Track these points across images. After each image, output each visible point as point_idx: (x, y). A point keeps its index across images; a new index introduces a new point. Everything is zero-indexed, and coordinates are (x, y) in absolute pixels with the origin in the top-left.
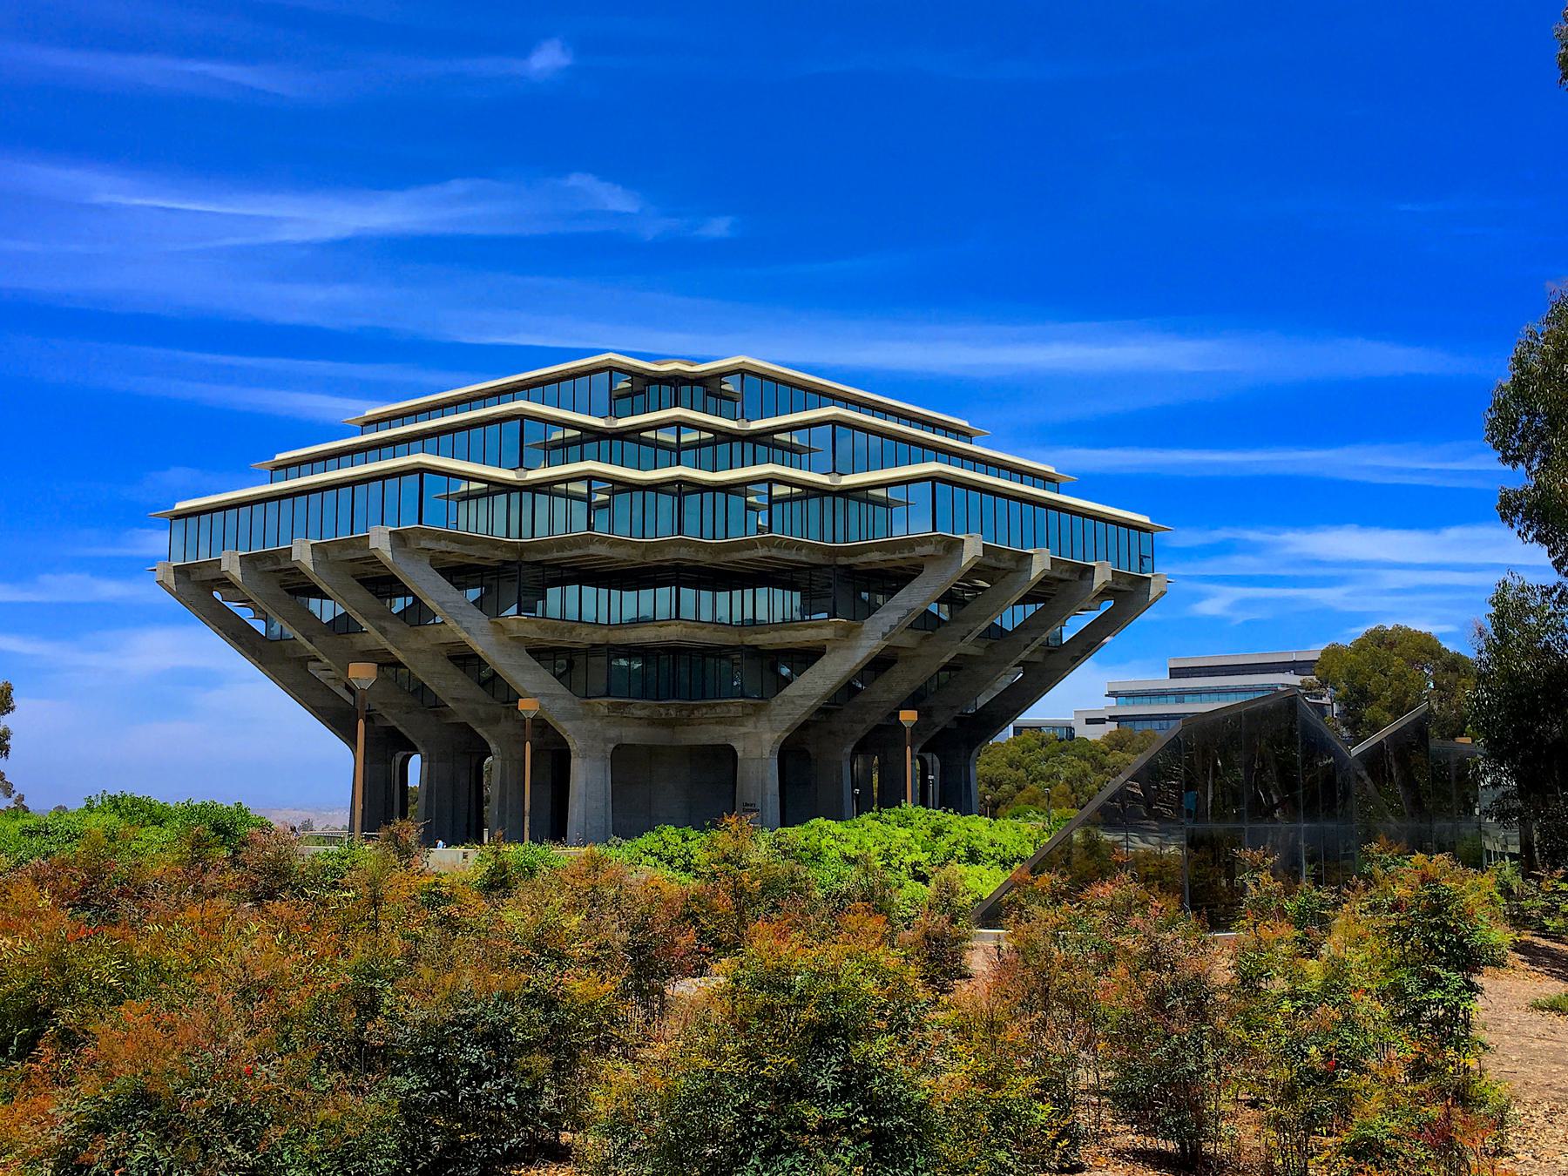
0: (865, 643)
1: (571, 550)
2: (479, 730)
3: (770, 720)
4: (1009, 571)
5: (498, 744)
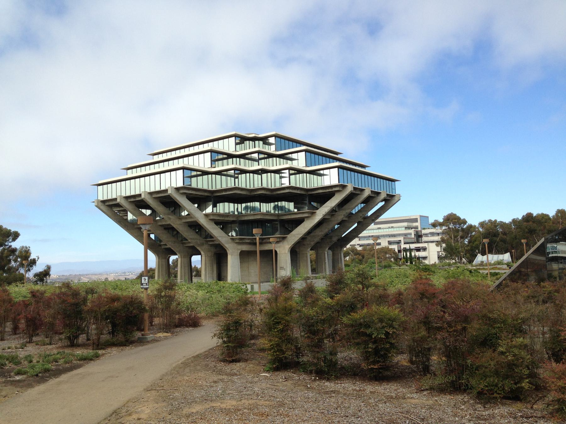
2: (198, 248)
4: (358, 194)
5: (204, 252)
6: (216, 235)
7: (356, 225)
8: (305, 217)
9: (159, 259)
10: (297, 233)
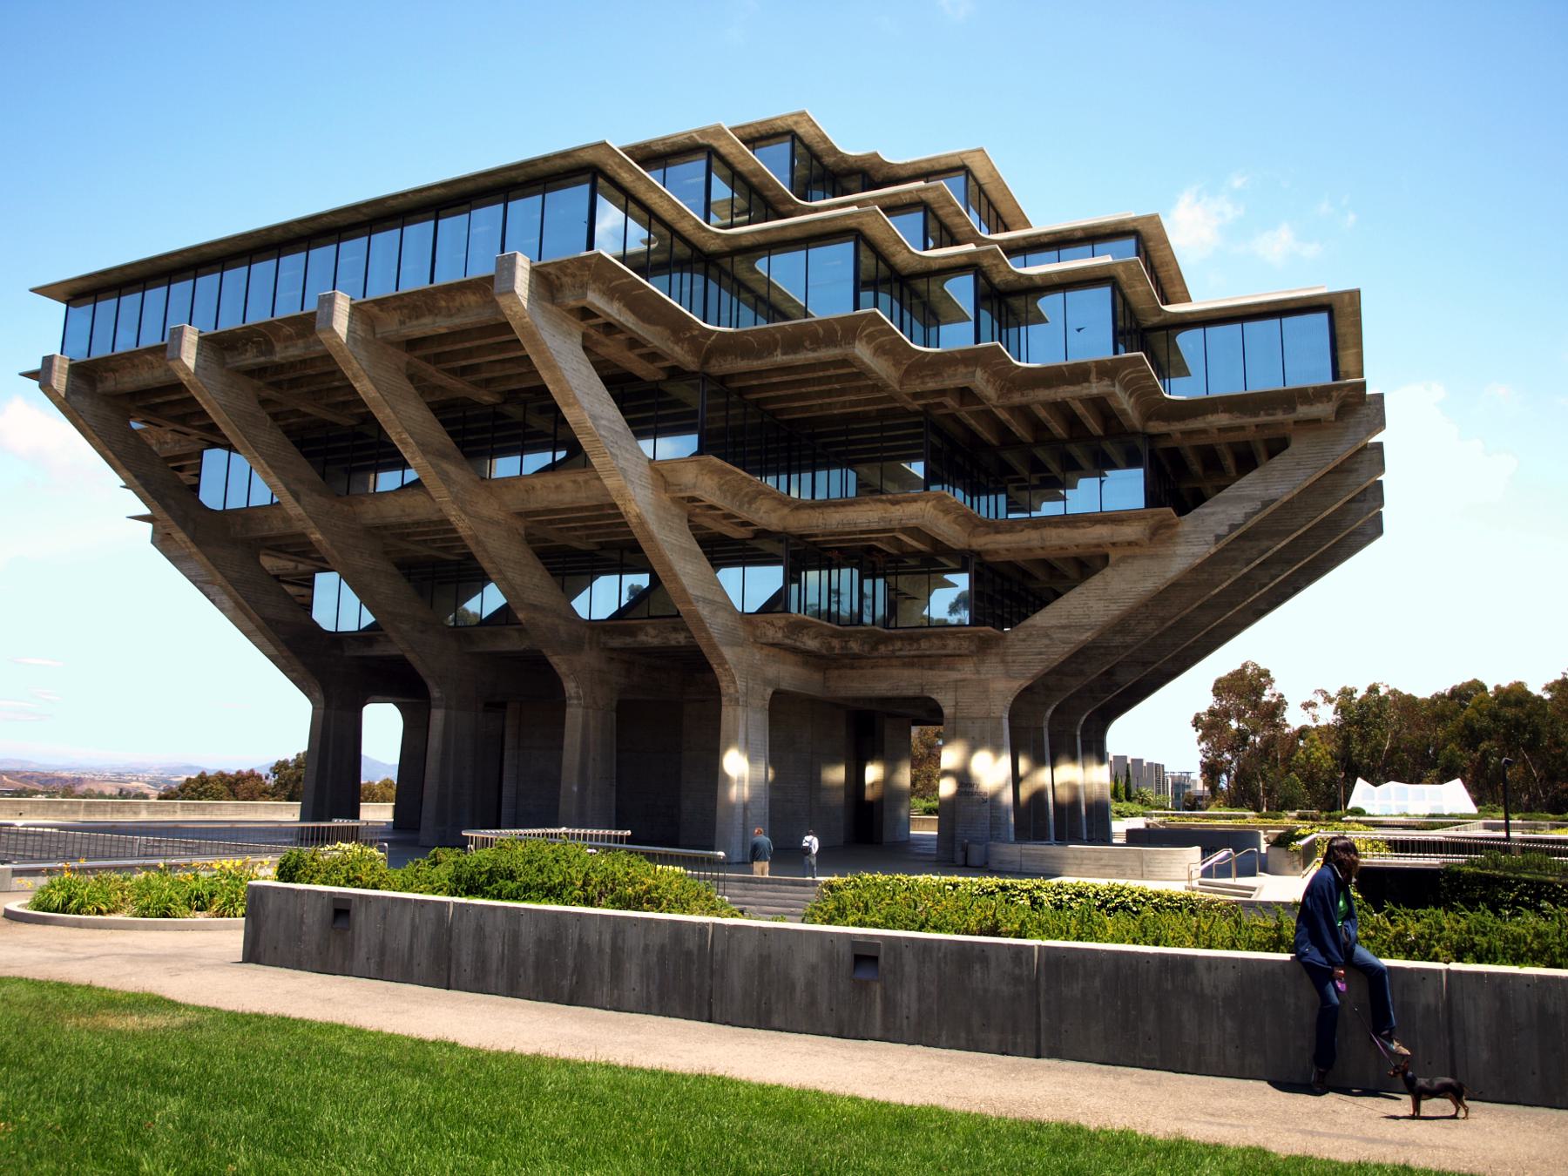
0: (1181, 549)
1: (814, 350)
3: (1003, 661)
9: (327, 706)
10: (1064, 622)
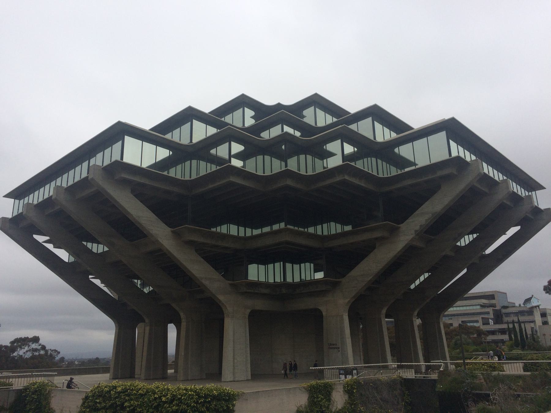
2: (174, 305)
6: (197, 275)
7: (465, 271)
8: (376, 239)
